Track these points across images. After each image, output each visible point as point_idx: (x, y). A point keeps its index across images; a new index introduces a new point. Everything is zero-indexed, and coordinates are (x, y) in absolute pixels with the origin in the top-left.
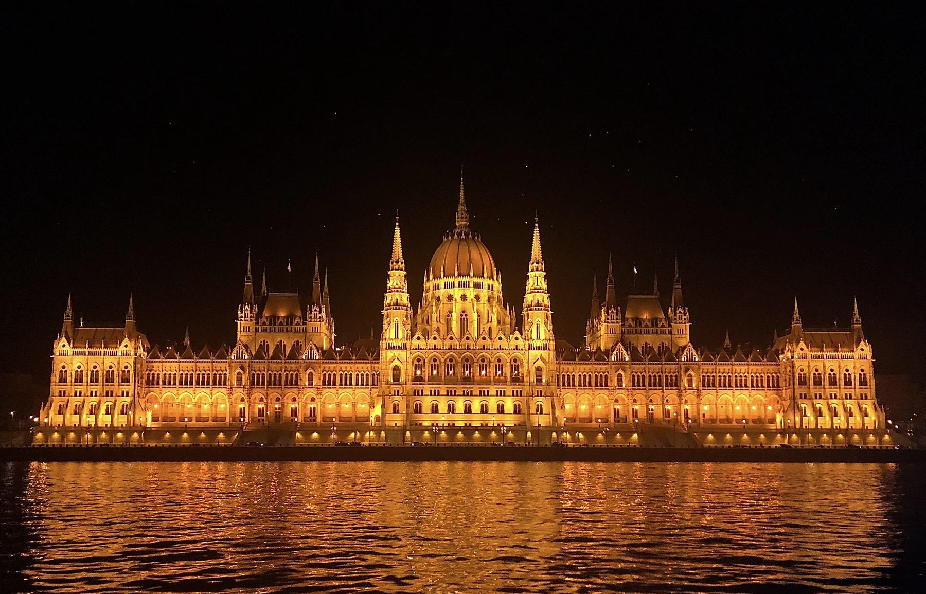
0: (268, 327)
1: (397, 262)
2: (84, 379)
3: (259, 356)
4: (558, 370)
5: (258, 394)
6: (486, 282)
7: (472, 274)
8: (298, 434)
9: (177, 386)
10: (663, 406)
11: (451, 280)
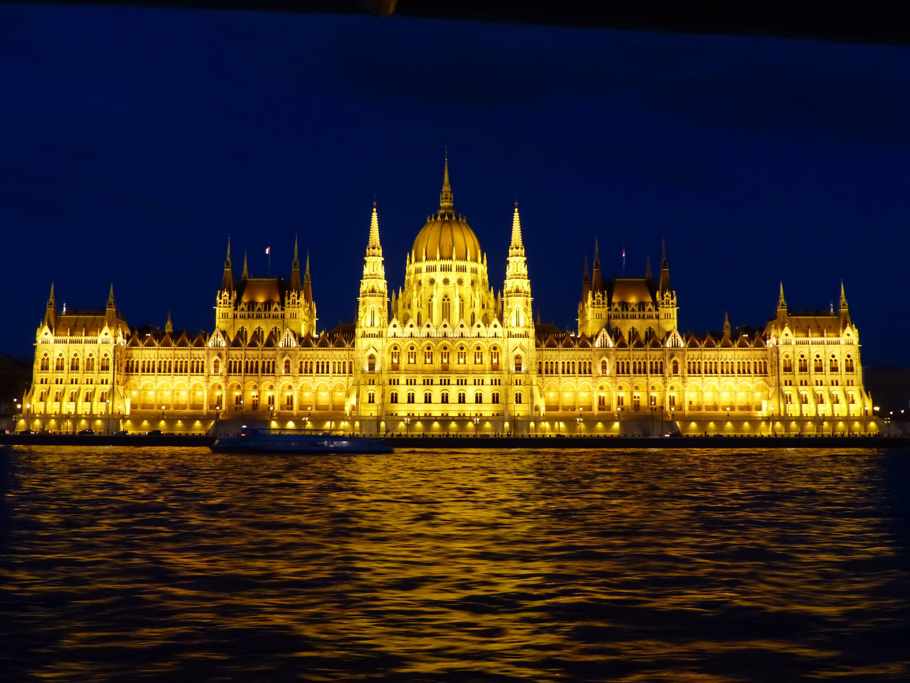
0: (247, 313)
1: (374, 248)
2: (66, 367)
4: (539, 357)
5: (235, 380)
6: (469, 265)
7: (454, 257)
10: (648, 394)
11: (432, 263)
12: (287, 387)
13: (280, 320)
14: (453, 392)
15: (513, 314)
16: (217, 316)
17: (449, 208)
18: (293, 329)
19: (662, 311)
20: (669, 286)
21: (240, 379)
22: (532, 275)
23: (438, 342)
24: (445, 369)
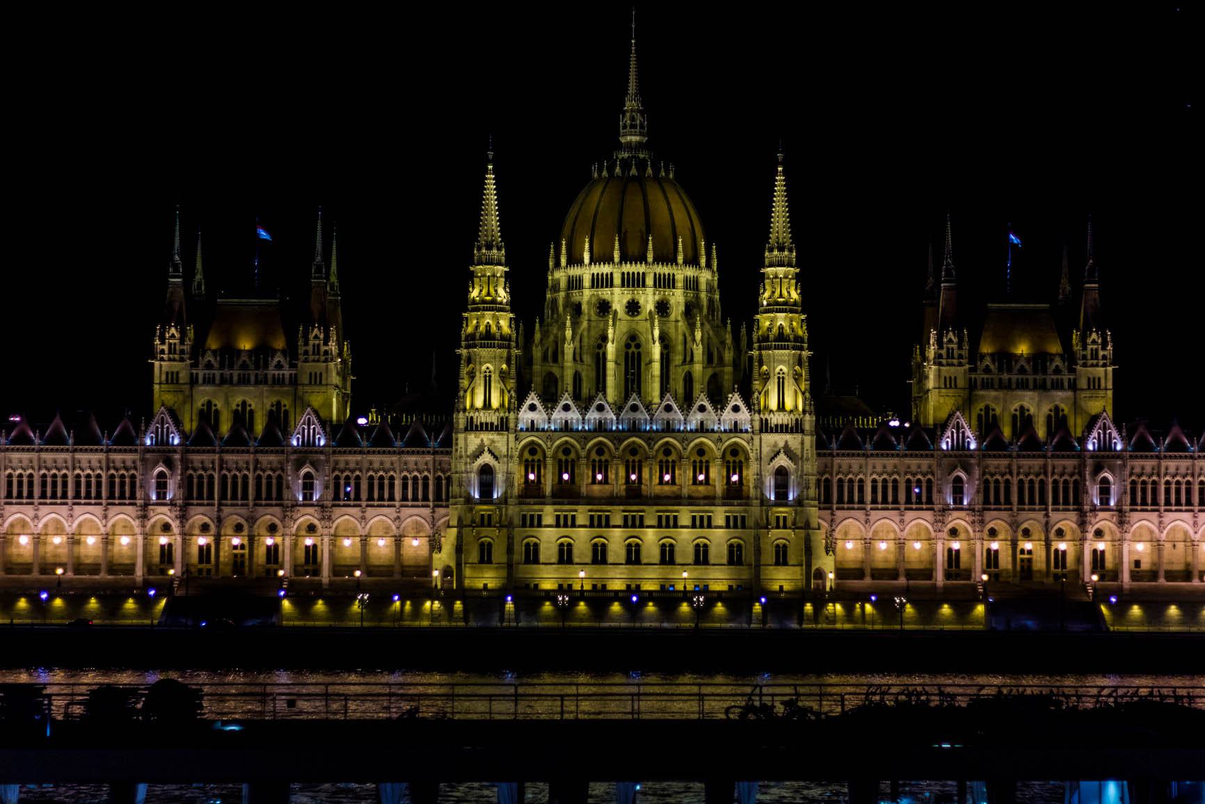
0: (217, 373)
1: (489, 247)
3: (202, 438)
5: (199, 516)
6: (682, 273)
7: (650, 259)
8: (286, 604)
9: (36, 501)
12: (304, 527)
15: (773, 388)
16: (157, 380)
17: (639, 146)
19: (1084, 373)
20: (1098, 321)
22: (807, 305)
23: (621, 441)
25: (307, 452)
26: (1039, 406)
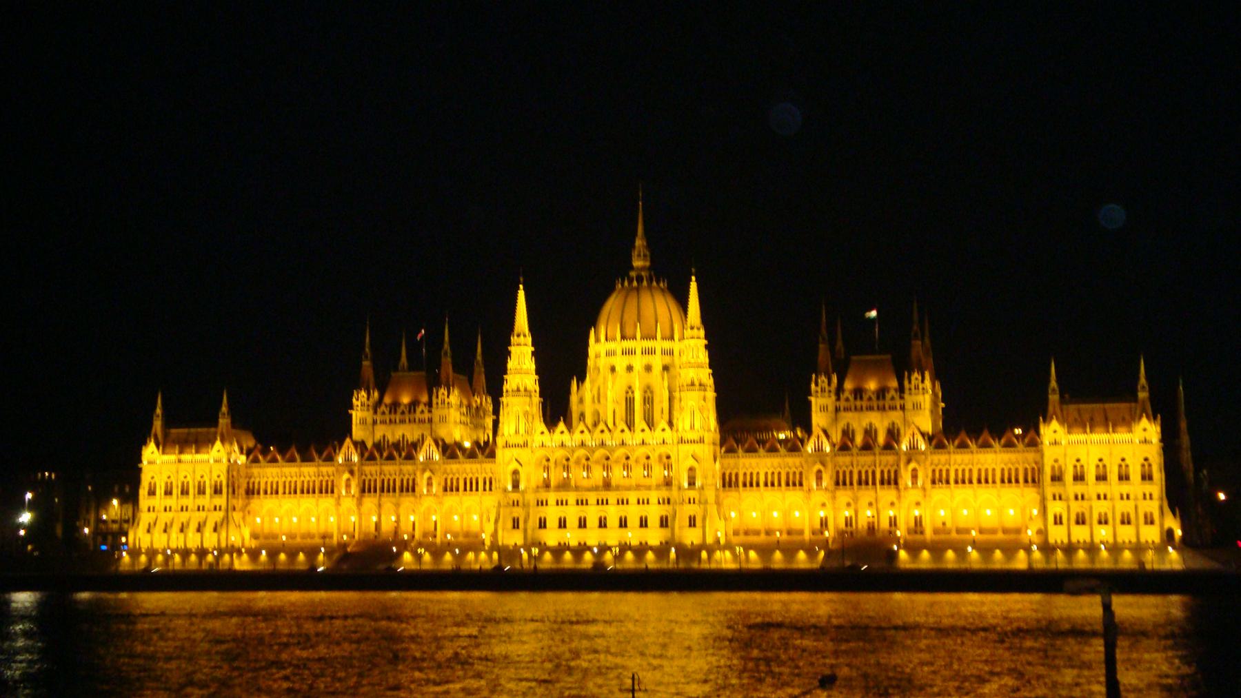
0: (387, 417)
1: (518, 336)
2: (174, 491)
5: (370, 502)
6: (659, 344)
7: (638, 336)
11: (611, 346)
13: (427, 425)
14: (613, 513)
17: (643, 268)
18: (442, 432)
19: (909, 400)
21: (376, 500)
24: (607, 485)
25: (428, 464)
26: (882, 421)
